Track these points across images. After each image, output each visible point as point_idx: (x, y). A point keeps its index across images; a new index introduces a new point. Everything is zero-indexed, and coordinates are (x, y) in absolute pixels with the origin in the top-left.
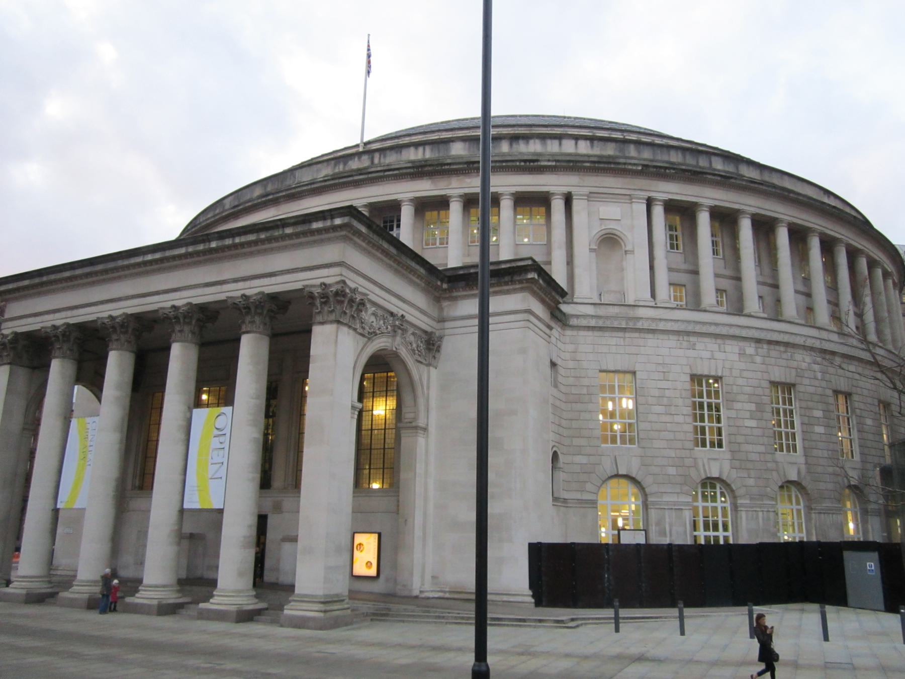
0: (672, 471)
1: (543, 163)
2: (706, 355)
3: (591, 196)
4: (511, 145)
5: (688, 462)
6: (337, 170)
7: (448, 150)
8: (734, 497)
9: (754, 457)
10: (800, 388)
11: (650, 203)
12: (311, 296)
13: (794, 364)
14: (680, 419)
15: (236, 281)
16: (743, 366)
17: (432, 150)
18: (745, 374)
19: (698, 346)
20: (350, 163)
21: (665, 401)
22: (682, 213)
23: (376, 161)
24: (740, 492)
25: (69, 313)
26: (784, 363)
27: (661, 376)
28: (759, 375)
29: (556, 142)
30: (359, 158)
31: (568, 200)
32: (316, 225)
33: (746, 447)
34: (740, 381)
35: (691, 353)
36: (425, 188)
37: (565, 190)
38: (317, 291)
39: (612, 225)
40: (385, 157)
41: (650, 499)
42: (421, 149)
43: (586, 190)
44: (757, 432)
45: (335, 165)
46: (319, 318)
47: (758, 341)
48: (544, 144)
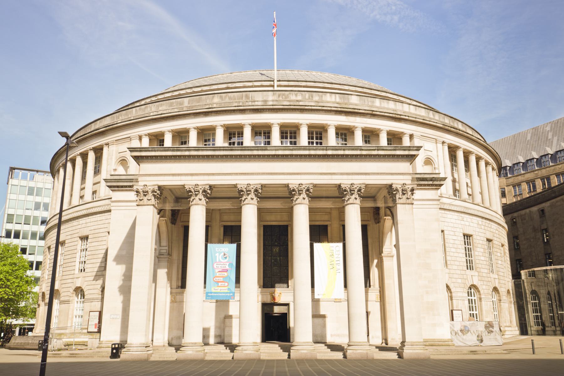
0: (460, 281)
2: (467, 224)
4: (381, 104)
5: (465, 277)
8: (480, 294)
9: (484, 275)
10: (494, 242)
12: (397, 190)
13: (492, 230)
14: (461, 255)
15: (342, 174)
16: (478, 230)
17: (340, 98)
18: (480, 234)
19: (465, 219)
21: (455, 246)
22: (453, 151)
24: (482, 292)
25: (206, 177)
26: (489, 229)
27: (452, 233)
28: (483, 235)
30: (296, 95)
33: (482, 270)
34: (478, 238)
35: (463, 222)
37: (411, 132)
38: (399, 187)
39: (429, 153)
41: (453, 295)
44: (485, 263)
47: (483, 218)
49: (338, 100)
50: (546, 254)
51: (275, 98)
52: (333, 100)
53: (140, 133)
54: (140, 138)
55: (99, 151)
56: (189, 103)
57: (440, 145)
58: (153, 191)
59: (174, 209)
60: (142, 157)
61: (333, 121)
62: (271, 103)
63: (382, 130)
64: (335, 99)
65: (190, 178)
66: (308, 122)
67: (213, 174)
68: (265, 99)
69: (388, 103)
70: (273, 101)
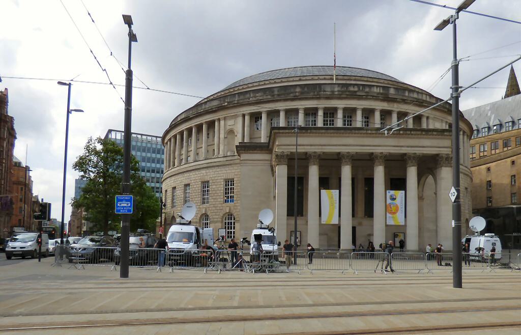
1: (424, 104)
3: (435, 119)
6: (343, 89)
7: (388, 91)
11: (446, 122)
12: (442, 157)
15: (408, 147)
17: (383, 90)
20: (350, 87)
23: (361, 89)
25: (320, 147)
29: (421, 95)
30: (354, 87)
31: (428, 118)
32: (445, 134)
36: (385, 106)
37: (427, 115)
38: (444, 156)
40: (365, 88)
42: (379, 88)
43: (432, 116)
45: (342, 87)
46: (444, 165)
48: (418, 95)
49: (381, 91)
50: (487, 198)
51: (339, 89)
52: (378, 91)
53: (244, 113)
54: (244, 116)
55: (211, 125)
56: (278, 92)
57: (444, 124)
58: (287, 155)
59: (297, 165)
60: (280, 133)
61: (379, 105)
62: (336, 93)
63: (410, 113)
64: (380, 90)
65: (309, 147)
66: (362, 107)
67: (325, 145)
68: (332, 90)
69: (413, 94)
70: (338, 91)
